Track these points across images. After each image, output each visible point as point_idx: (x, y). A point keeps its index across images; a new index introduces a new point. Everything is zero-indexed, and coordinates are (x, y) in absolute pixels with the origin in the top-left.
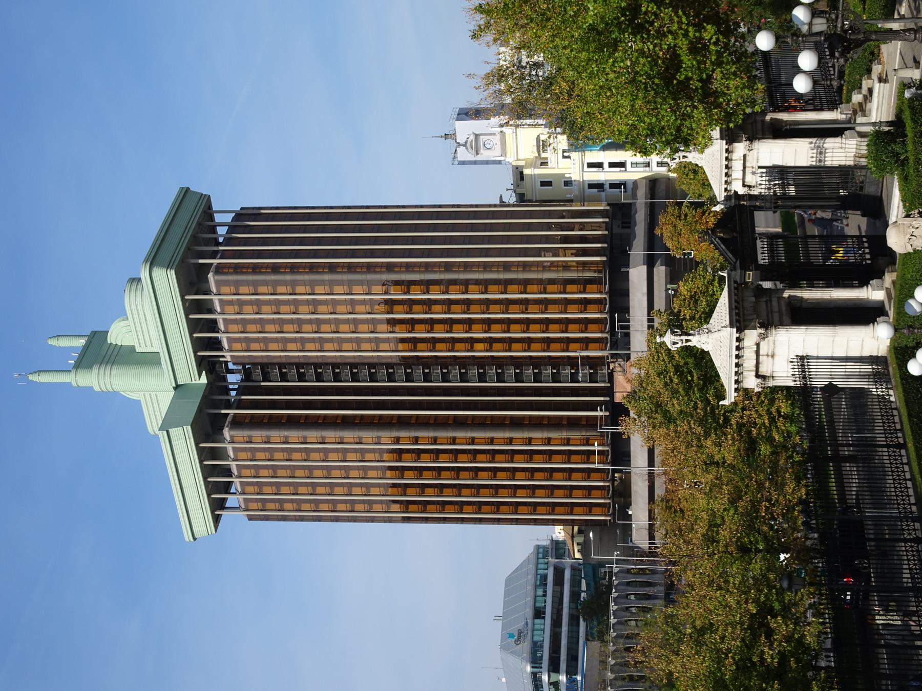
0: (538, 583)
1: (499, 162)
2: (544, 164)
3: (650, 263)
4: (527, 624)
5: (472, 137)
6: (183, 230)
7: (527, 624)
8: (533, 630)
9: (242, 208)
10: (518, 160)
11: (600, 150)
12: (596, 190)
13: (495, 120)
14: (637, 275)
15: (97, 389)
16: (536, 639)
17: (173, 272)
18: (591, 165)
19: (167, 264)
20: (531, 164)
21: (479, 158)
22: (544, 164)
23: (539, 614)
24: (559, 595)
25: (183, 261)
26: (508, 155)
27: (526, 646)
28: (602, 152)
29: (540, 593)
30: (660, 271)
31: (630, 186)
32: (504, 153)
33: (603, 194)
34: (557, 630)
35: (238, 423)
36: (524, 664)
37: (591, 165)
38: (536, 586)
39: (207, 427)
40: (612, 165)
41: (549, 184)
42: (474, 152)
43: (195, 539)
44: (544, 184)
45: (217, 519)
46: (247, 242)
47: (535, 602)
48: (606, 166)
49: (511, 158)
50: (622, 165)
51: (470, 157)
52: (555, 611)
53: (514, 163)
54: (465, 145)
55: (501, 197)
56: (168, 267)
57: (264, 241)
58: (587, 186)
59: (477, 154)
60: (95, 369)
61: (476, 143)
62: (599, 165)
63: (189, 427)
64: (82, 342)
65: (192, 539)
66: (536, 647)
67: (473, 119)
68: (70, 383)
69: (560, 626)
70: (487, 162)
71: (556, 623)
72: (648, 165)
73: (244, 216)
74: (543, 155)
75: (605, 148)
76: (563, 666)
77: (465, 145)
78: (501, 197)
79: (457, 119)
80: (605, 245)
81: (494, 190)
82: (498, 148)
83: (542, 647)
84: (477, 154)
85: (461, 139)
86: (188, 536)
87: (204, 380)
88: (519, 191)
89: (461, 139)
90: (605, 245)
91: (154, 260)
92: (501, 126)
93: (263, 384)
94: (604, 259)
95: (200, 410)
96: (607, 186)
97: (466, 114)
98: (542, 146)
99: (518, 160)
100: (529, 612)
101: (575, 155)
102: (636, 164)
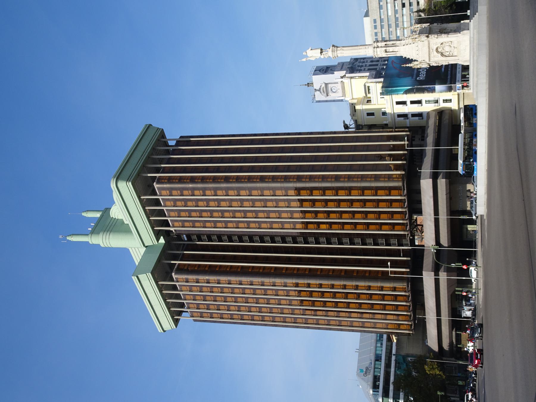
0: (378, 338)
1: (342, 100)
2: (369, 101)
3: (435, 177)
4: (371, 363)
5: (323, 85)
6: (142, 153)
7: (371, 363)
8: (375, 368)
9: (181, 137)
10: (353, 99)
11: (404, 93)
12: (402, 118)
13: (338, 74)
14: (426, 185)
15: (102, 245)
16: (376, 374)
17: (130, 183)
18: (398, 103)
19: (127, 178)
20: (361, 102)
21: (328, 98)
22: (369, 101)
23: (378, 358)
24: (389, 348)
25: (138, 174)
26: (347, 96)
27: (370, 377)
28: (405, 95)
29: (379, 345)
30: (442, 183)
31: (425, 116)
32: (344, 95)
33: (407, 121)
34: (388, 370)
35: (181, 270)
36: (369, 387)
37: (398, 103)
38: (377, 341)
39: (162, 271)
40: (412, 102)
41: (372, 114)
42: (325, 94)
43: (164, 331)
44: (369, 114)
45: (176, 322)
46: (179, 161)
47: (376, 350)
48: (408, 103)
49: (348, 98)
50: (419, 102)
51: (323, 98)
52: (387, 358)
53: (350, 102)
54: (319, 90)
55: (344, 122)
56: (128, 180)
57: (189, 161)
58: (396, 116)
59: (327, 95)
60: (101, 234)
61: (326, 89)
62: (404, 103)
63: (150, 274)
64: (100, 213)
65: (162, 331)
66: (376, 379)
67: (324, 74)
68: (88, 242)
69: (390, 367)
70: (334, 101)
71: (388, 365)
72: (437, 102)
73: (184, 141)
74: (369, 95)
75: (407, 92)
76: (391, 394)
77: (319, 90)
78: (344, 122)
79: (314, 75)
80: (405, 162)
81: (335, 121)
82: (340, 91)
83: (379, 379)
84: (327, 95)
85: (316, 86)
86: (160, 330)
87: (162, 241)
88: (355, 118)
89: (316, 86)
90: (405, 162)
91: (118, 178)
92: (342, 77)
93: (198, 243)
94: (403, 173)
95: (159, 260)
96: (410, 116)
97: (320, 71)
98: (367, 90)
99: (353, 99)
100: (373, 358)
101: (387, 97)
102: (429, 101)
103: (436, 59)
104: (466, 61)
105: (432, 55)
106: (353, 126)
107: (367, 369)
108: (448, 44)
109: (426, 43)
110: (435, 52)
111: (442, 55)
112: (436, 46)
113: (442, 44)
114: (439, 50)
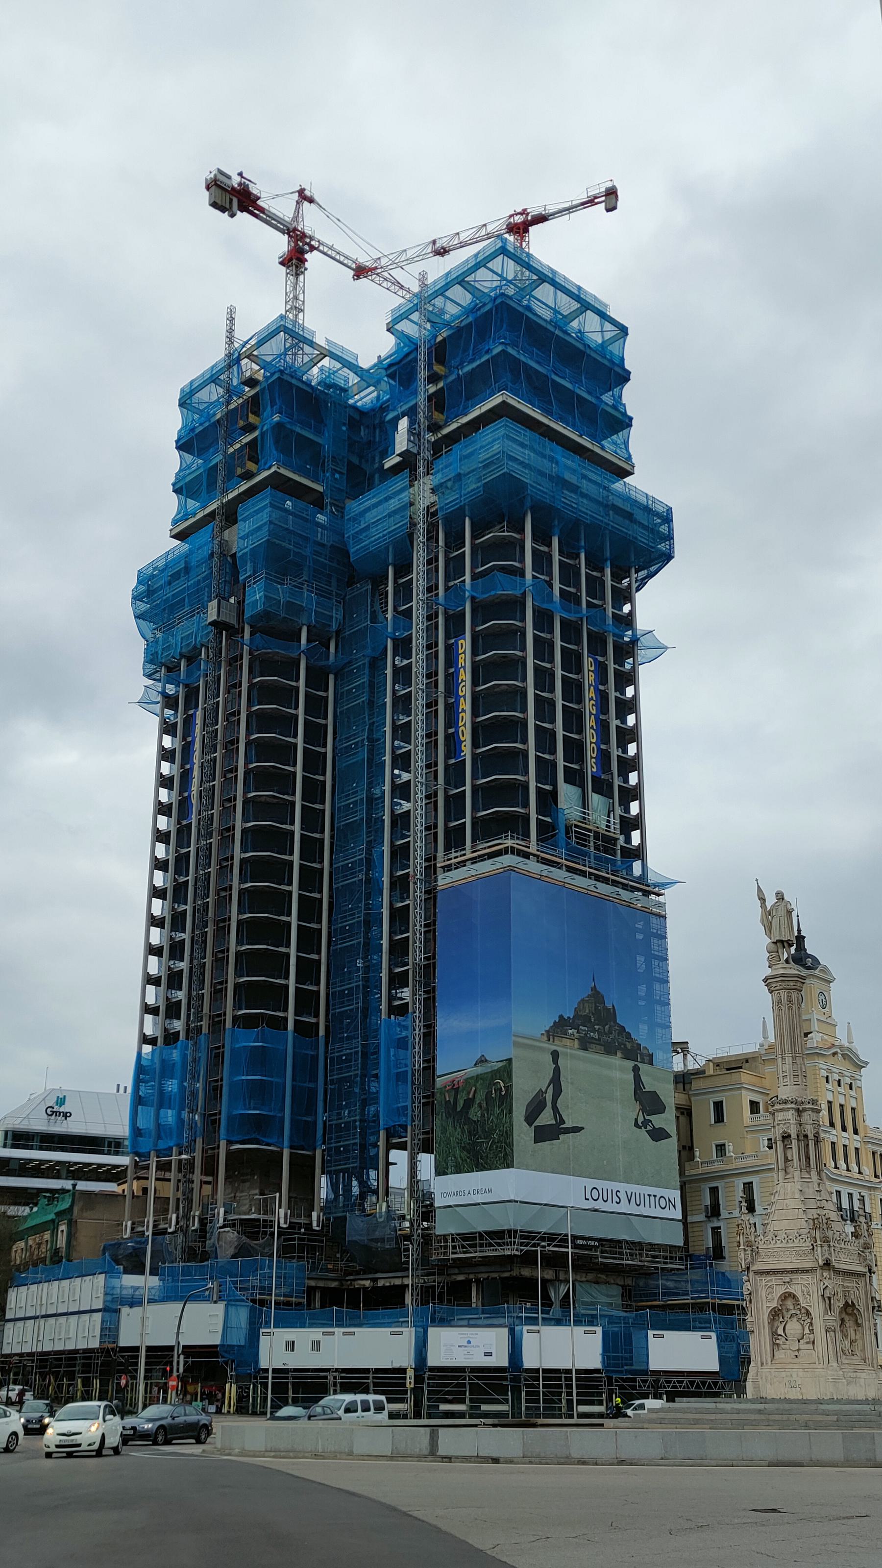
33: (702, 1217)
41: (719, 1118)
44: (718, 1106)
103: (763, 1293)
104: (756, 1387)
105: (773, 1280)
106: (692, 1066)
107: (66, 1115)
108: (807, 1331)
109: (808, 1265)
110: (781, 1290)
111: (776, 1314)
112: (799, 1295)
113: (808, 1313)
114: (789, 1303)
